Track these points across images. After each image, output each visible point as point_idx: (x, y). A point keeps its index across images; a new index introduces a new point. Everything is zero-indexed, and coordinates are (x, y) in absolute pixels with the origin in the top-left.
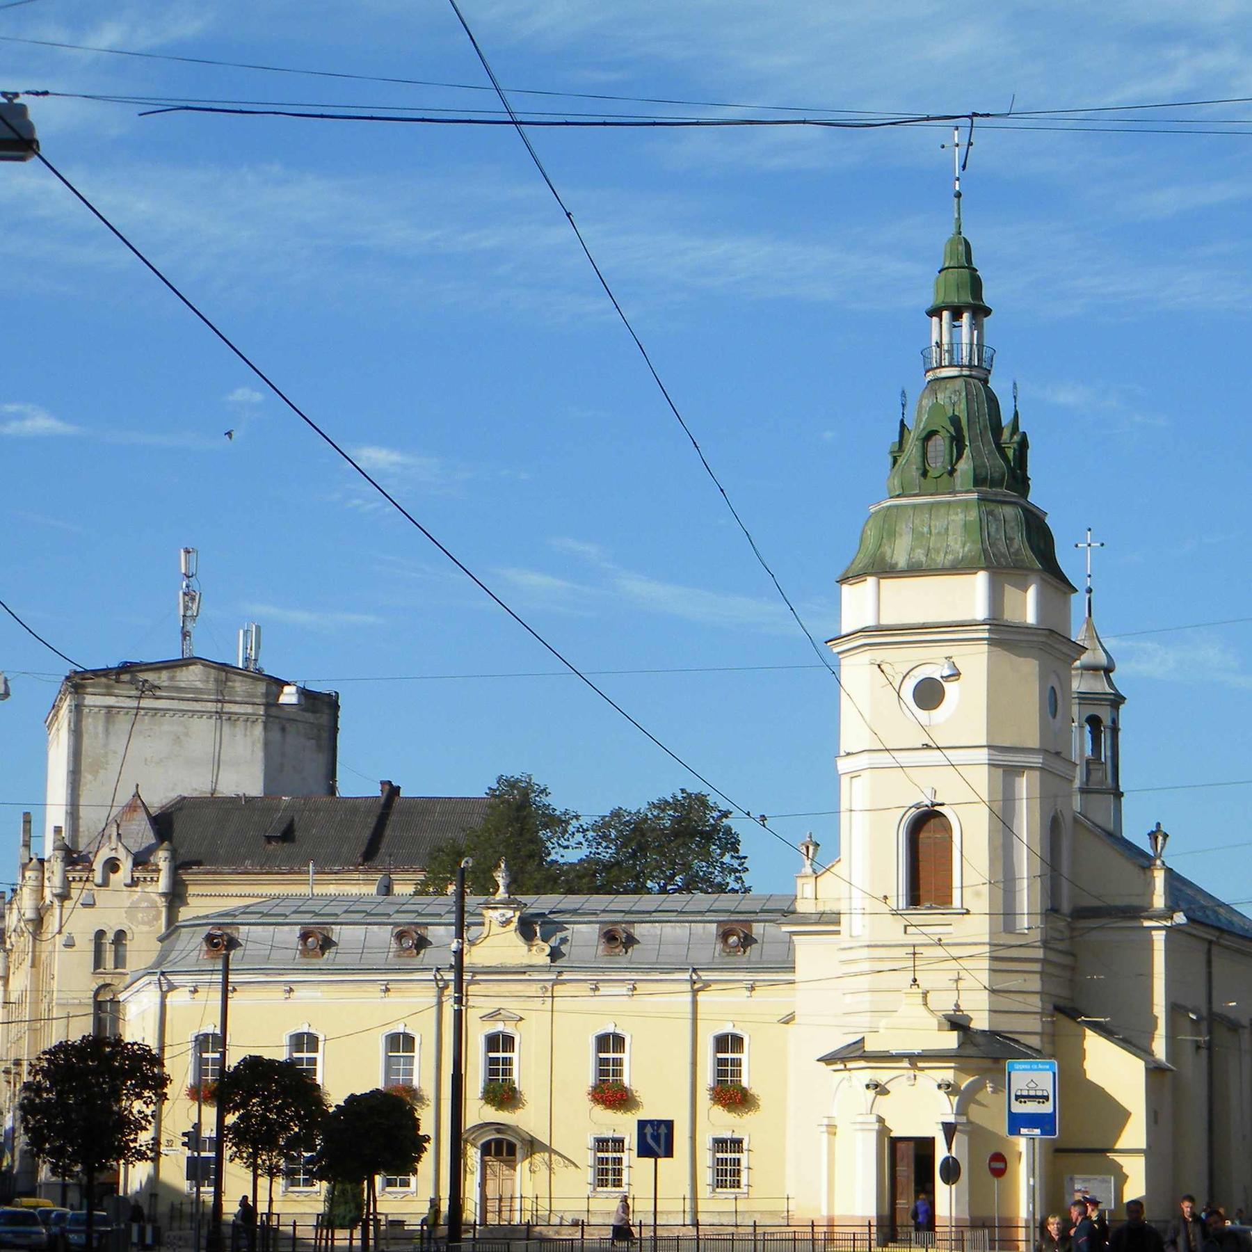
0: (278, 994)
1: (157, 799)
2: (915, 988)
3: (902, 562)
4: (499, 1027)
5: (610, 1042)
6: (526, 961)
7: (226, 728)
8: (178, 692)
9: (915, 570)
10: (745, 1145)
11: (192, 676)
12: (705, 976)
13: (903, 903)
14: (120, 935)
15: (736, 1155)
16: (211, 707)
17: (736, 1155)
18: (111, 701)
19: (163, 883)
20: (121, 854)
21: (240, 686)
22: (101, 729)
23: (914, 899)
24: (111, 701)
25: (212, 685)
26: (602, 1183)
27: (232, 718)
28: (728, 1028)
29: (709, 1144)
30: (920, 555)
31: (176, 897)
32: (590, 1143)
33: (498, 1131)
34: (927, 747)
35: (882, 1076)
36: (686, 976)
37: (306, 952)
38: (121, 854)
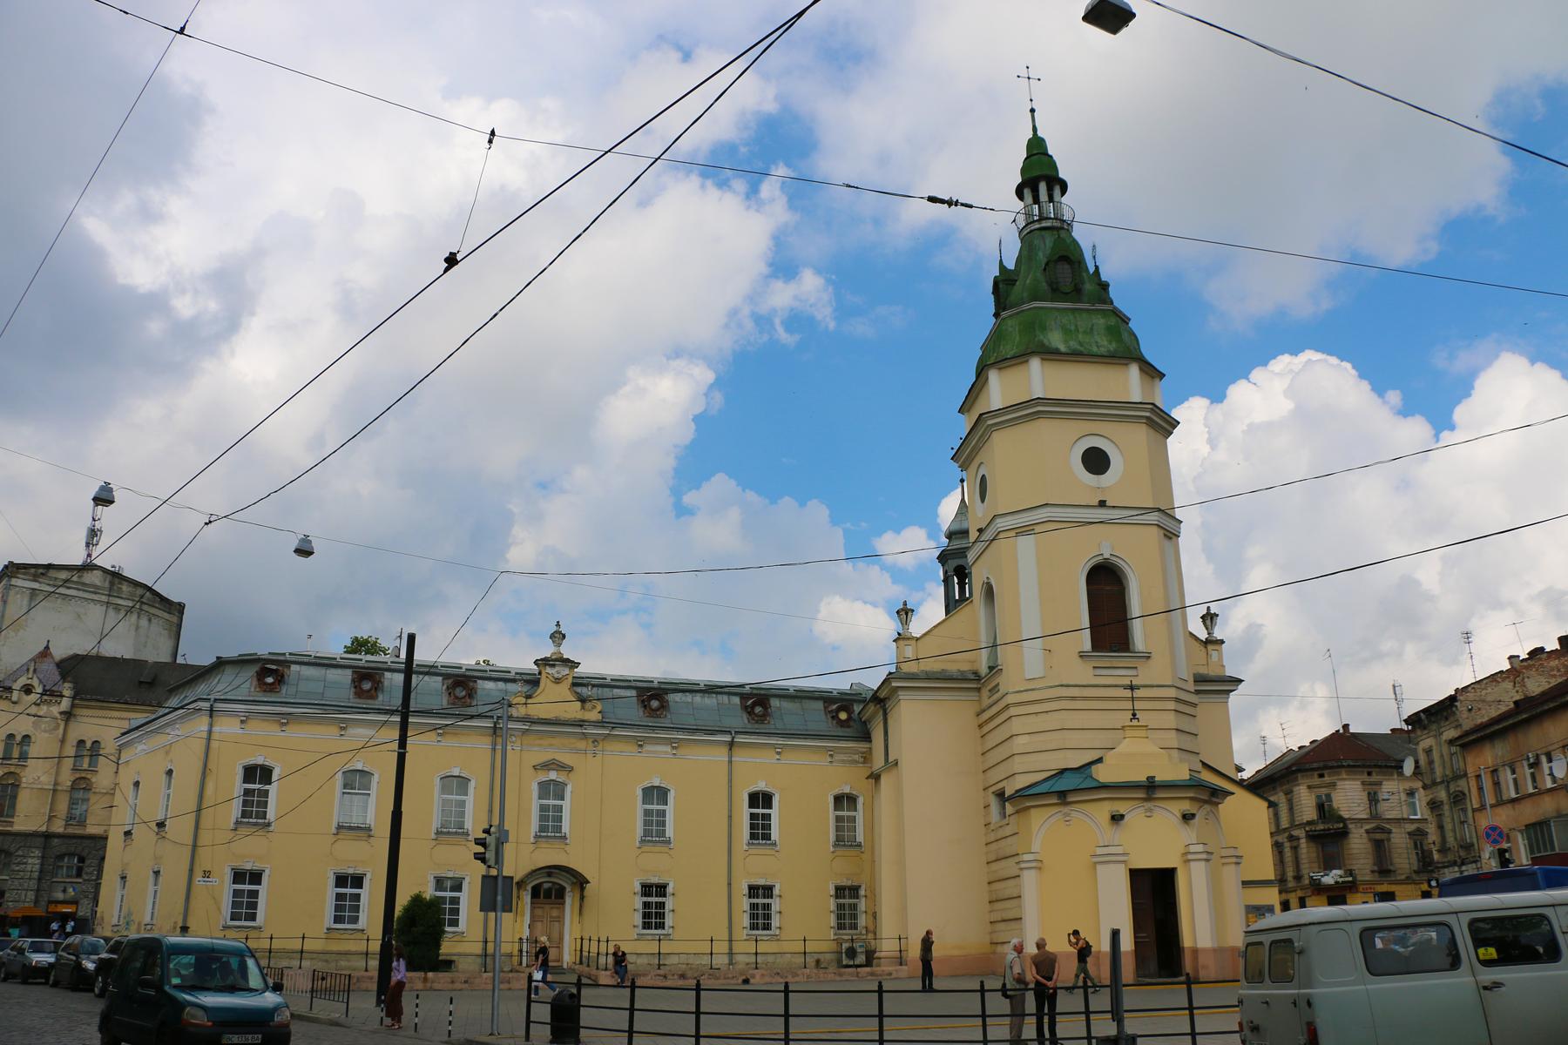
0: (333, 730)
1: (60, 652)
2: (1135, 722)
3: (1063, 348)
4: (553, 775)
5: (656, 794)
6: (580, 715)
7: (111, 612)
8: (83, 586)
9: (1077, 356)
10: (776, 891)
11: (94, 578)
12: (739, 739)
13: (1088, 646)
14: (26, 737)
15: (766, 901)
16: (104, 598)
17: (766, 901)
18: (35, 585)
19: (65, 704)
20: (35, 682)
21: (125, 587)
22: (25, 602)
23: (1097, 644)
24: (35, 585)
25: (107, 585)
26: (646, 926)
27: (117, 608)
28: (761, 786)
29: (746, 891)
30: (1074, 344)
31: (68, 716)
32: (638, 888)
33: (549, 875)
34: (1102, 504)
35: (1121, 808)
36: (728, 738)
37: (360, 693)
38: (35, 682)
